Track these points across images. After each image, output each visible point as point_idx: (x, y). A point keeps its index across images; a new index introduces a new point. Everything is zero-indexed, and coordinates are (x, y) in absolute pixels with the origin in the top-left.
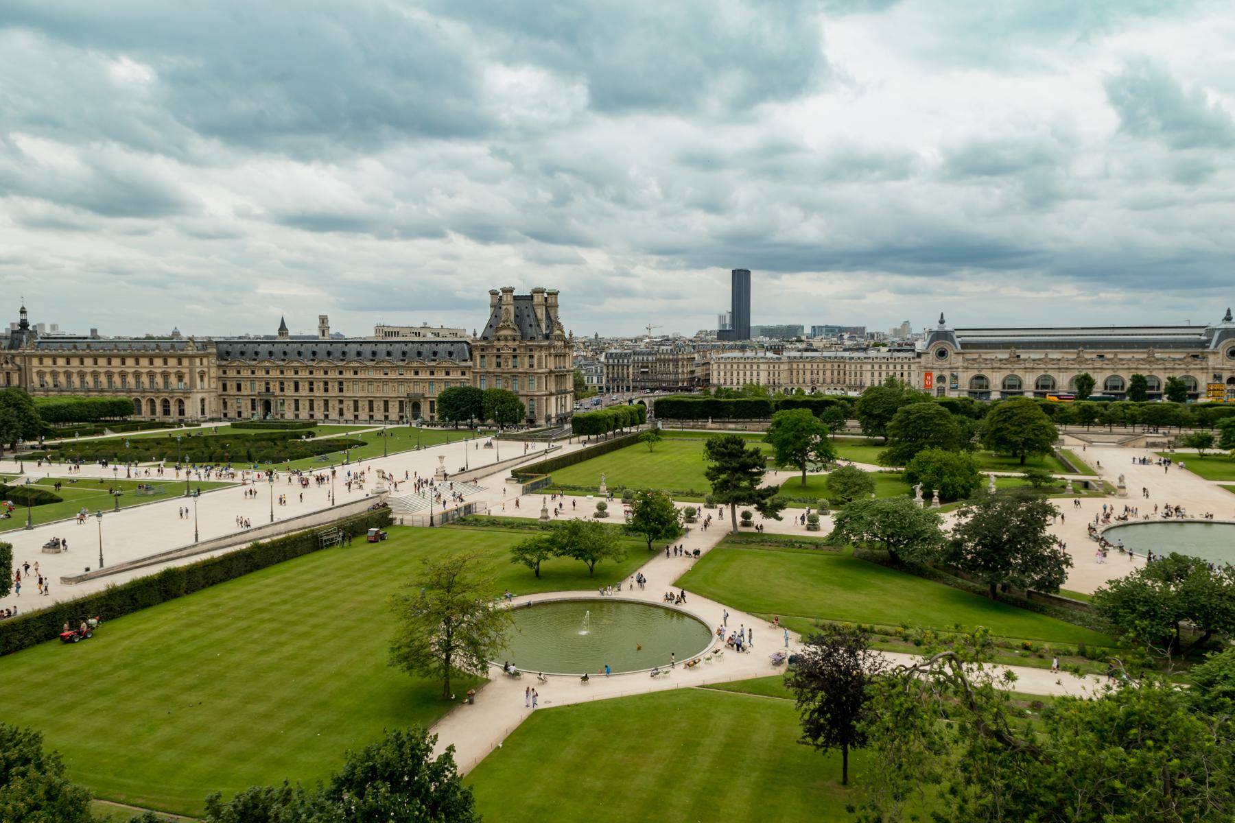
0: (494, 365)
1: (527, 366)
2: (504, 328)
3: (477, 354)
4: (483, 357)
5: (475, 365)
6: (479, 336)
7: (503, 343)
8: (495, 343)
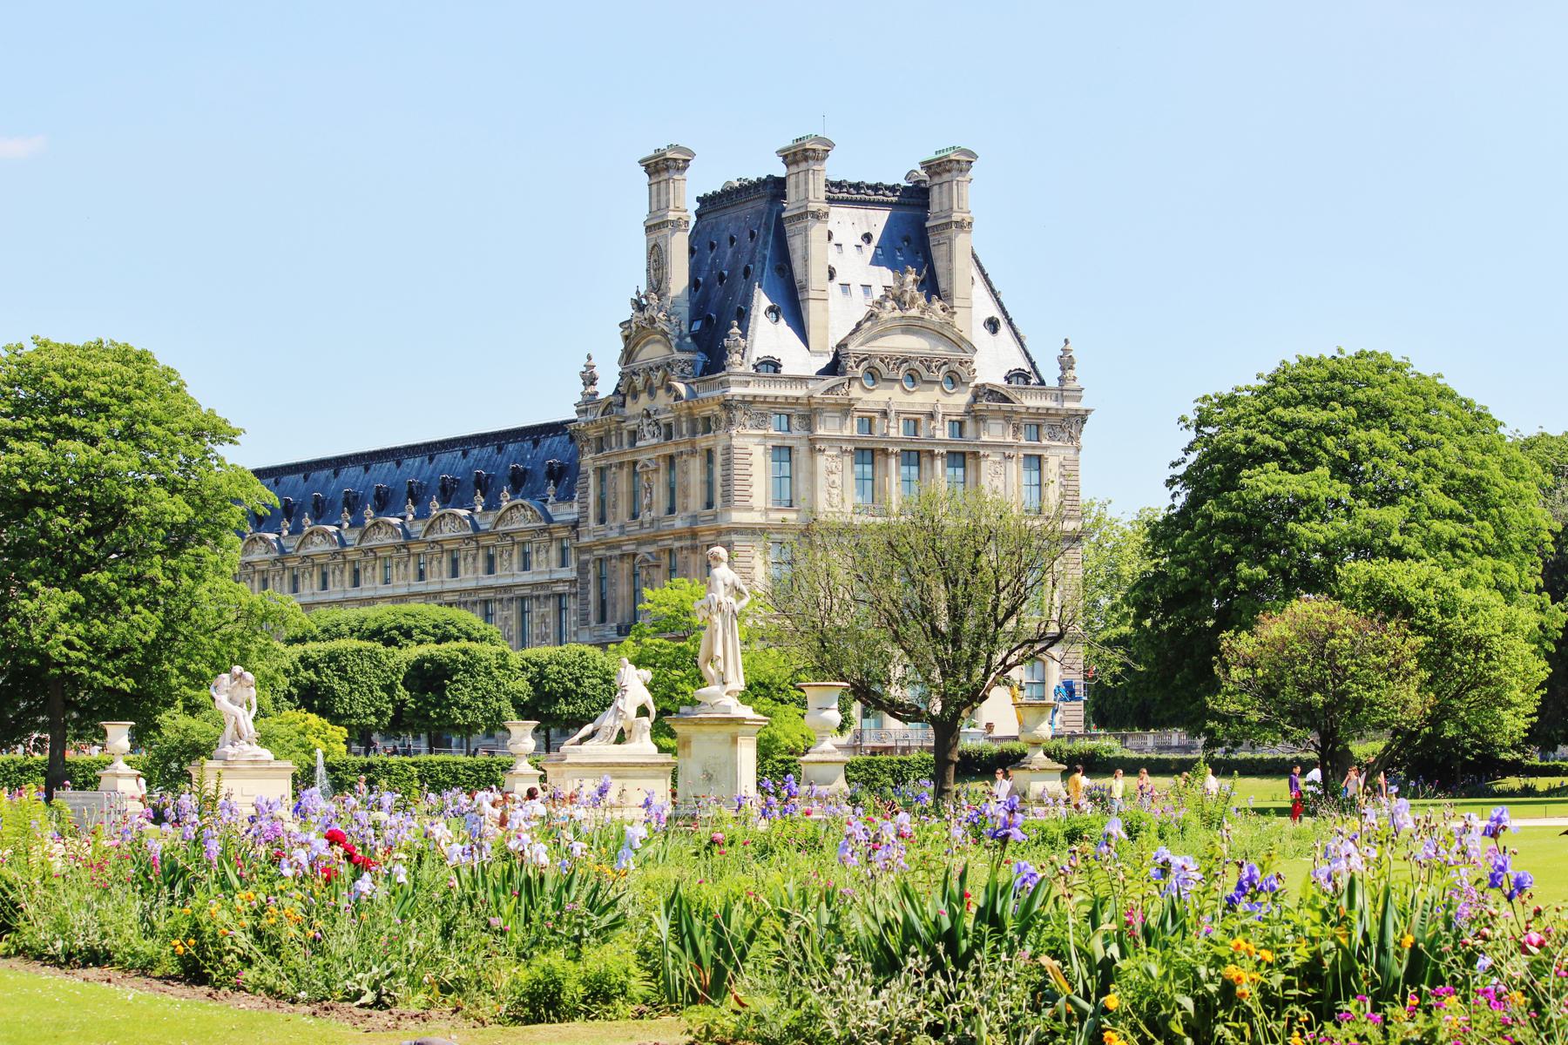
1: (695, 502)
6: (606, 387)
7: (644, 398)
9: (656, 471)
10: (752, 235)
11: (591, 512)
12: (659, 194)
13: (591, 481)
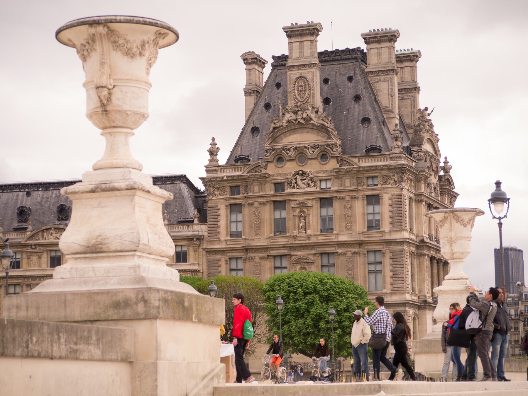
0: (267, 230)
2: (295, 127)
3: (219, 202)
4: (235, 208)
5: (214, 232)
6: (223, 158)
8: (271, 169)
9: (311, 207)
10: (350, 79)
11: (223, 230)
12: (301, 48)
13: (223, 211)
